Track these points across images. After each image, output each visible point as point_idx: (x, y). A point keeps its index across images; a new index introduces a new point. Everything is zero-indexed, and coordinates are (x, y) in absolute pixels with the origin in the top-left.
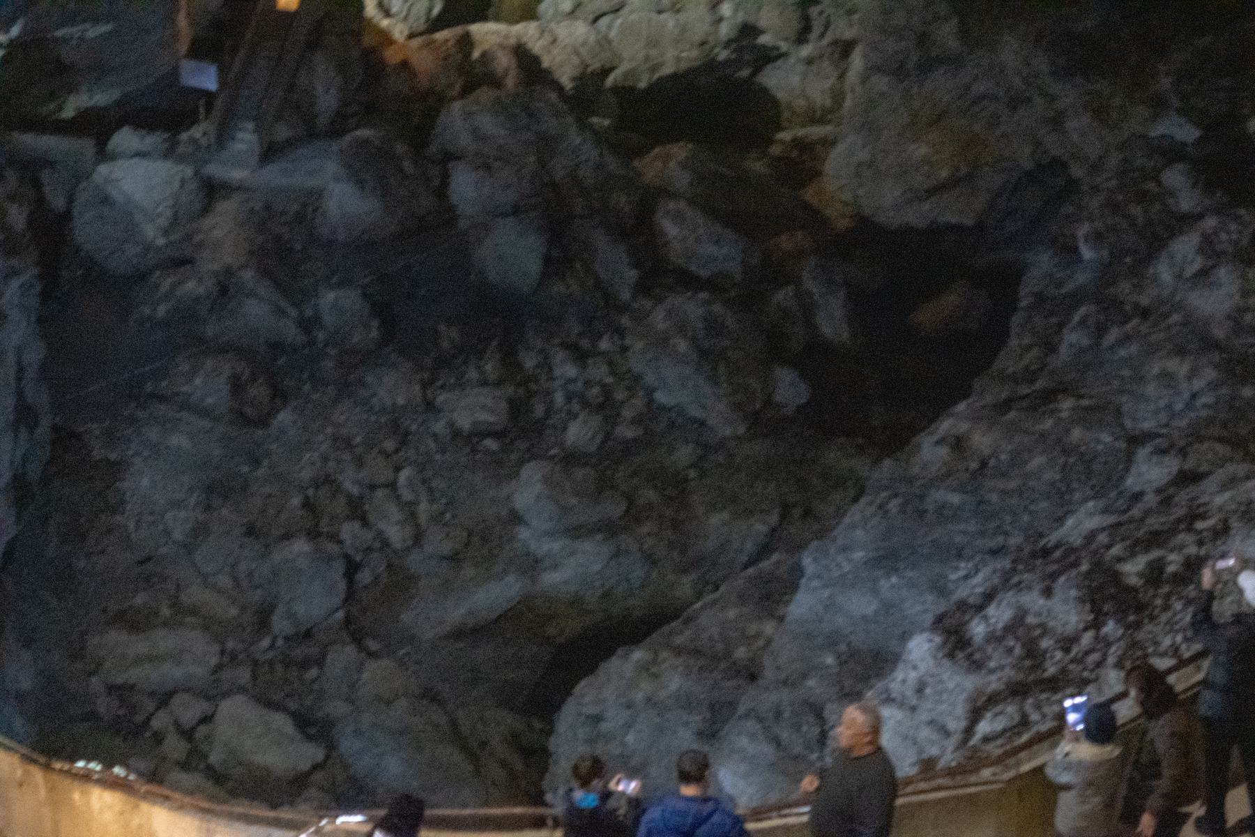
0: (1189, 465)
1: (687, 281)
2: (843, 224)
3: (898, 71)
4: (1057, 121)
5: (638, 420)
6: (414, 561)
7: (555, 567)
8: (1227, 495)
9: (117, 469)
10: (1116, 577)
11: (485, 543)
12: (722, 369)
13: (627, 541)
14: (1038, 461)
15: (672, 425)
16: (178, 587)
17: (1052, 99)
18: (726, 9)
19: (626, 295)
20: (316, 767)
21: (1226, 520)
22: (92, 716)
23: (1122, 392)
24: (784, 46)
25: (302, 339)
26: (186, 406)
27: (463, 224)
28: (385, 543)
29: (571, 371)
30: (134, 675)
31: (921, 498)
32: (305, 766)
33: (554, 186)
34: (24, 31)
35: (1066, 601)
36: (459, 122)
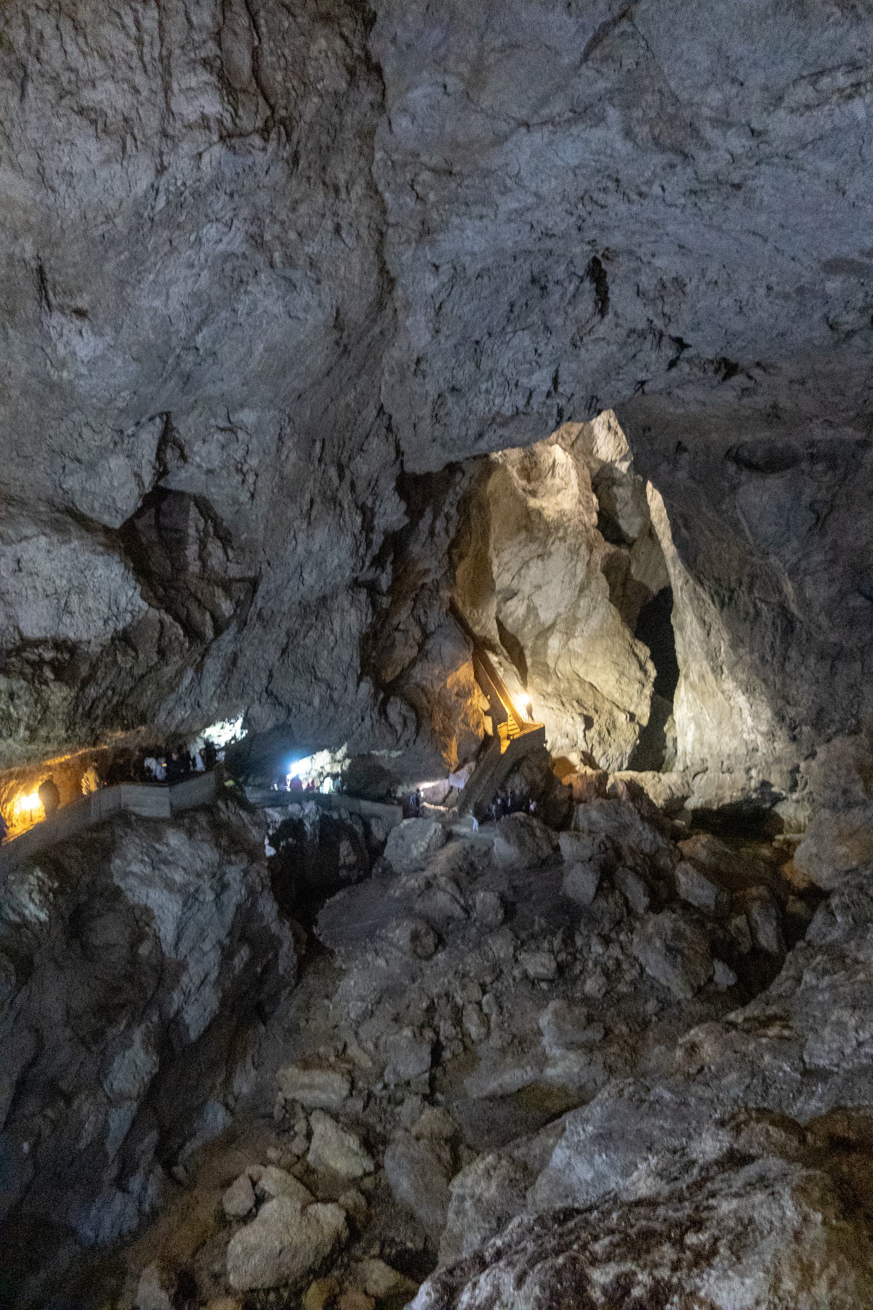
0: (740, 1144)
1: (686, 906)
2: (803, 885)
3: (834, 807)
5: (633, 983)
6: (482, 1050)
7: (554, 1065)
8: (735, 1203)
9: (342, 973)
10: (581, 1283)
11: (522, 1044)
12: (679, 959)
13: (598, 1057)
14: (733, 1076)
15: (652, 987)
16: (345, 1046)
18: (754, 773)
19: (641, 911)
20: (366, 1174)
21: (716, 1240)
22: (271, 1116)
23: (812, 1029)
25: (463, 915)
26: (392, 944)
28: (465, 1034)
29: (600, 950)
30: (300, 1095)
31: (648, 1090)
32: (359, 1172)
33: (617, 850)
35: (527, 1299)
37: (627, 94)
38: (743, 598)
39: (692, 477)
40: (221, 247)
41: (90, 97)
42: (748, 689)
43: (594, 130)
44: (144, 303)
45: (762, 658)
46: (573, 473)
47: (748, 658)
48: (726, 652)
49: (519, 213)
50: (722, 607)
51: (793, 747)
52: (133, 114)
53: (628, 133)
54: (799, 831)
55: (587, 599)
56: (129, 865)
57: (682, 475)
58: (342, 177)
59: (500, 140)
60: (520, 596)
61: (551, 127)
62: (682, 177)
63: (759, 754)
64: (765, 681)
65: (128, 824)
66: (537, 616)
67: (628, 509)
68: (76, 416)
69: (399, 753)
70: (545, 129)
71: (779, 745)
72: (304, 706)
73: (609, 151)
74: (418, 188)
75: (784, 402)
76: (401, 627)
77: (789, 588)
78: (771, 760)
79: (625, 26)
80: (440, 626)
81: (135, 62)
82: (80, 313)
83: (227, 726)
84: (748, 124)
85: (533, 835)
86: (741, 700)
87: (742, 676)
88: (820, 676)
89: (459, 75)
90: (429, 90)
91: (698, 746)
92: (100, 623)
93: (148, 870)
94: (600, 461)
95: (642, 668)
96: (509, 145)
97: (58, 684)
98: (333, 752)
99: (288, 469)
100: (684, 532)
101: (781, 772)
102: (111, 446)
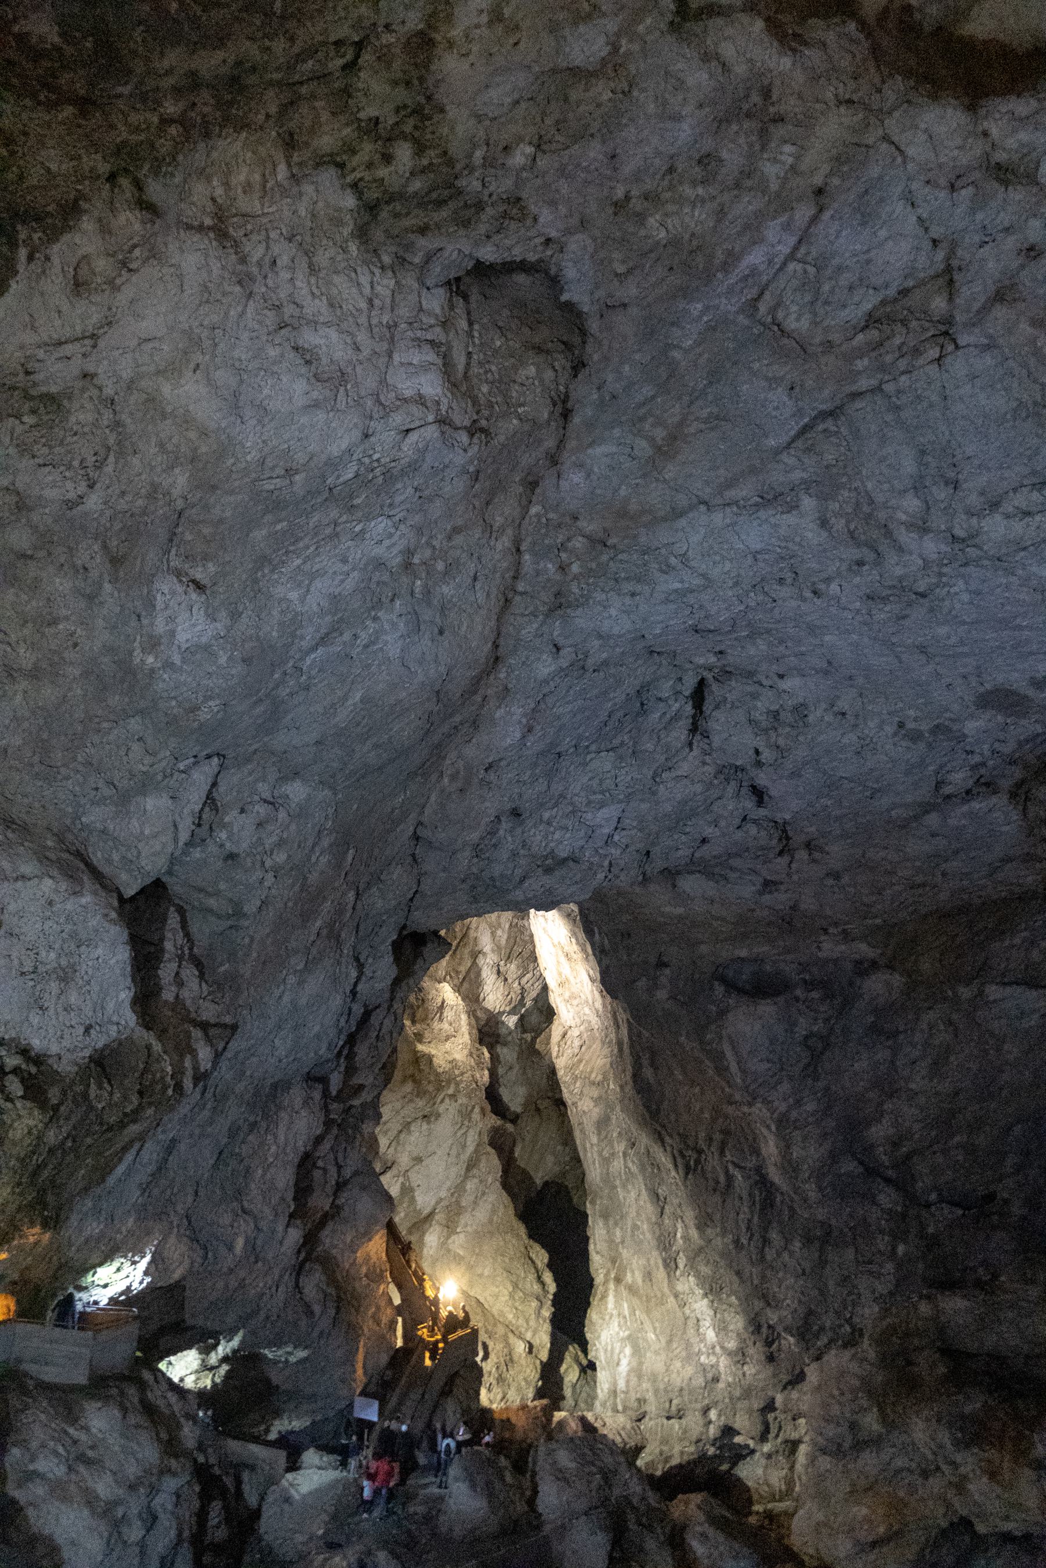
4: (960, 1486)
17: (953, 1464)
18: (713, 1415)
24: (751, 1443)
27: (547, 1528)
34: (242, 1342)
36: (541, 1459)
37: (824, 486)
38: (712, 1162)
39: (673, 998)
40: (379, 551)
41: (309, 338)
42: (713, 1290)
43: (784, 516)
44: (279, 591)
45: (737, 1242)
46: (464, 1017)
47: (718, 1242)
48: (686, 1238)
49: (681, 593)
50: (687, 1174)
51: (769, 1370)
52: (349, 370)
53: (824, 523)
54: (773, 1499)
55: (476, 1181)
56: (32, 1460)
57: (661, 994)
58: (499, 520)
59: (677, 514)
60: (394, 1171)
61: (735, 509)
62: (869, 577)
63: (721, 1385)
64: (738, 1273)
65: (24, 1391)
66: (413, 1200)
67: (513, 1075)
68: (134, 724)
69: (302, 1354)
70: (728, 510)
71: (750, 1370)
72: (223, 1250)
73: (797, 539)
74: (563, 555)
75: (809, 904)
76: (320, 1163)
77: (770, 1148)
78: (737, 1393)
79: (829, 424)
80: (356, 1173)
81: (363, 320)
82: (199, 587)
83: (127, 1268)
84: (949, 530)
85: (502, 1479)
86: (701, 1306)
87: (706, 1270)
88: (807, 1265)
89: (651, 440)
90: (614, 449)
91: (634, 1381)
92: (82, 1030)
93: (61, 1471)
94: (487, 1010)
95: (539, 1279)
96: (683, 522)
97: (28, 1104)
98: (206, 1351)
99: (313, 878)
100: (648, 1073)
101: (750, 1411)
102: (159, 777)
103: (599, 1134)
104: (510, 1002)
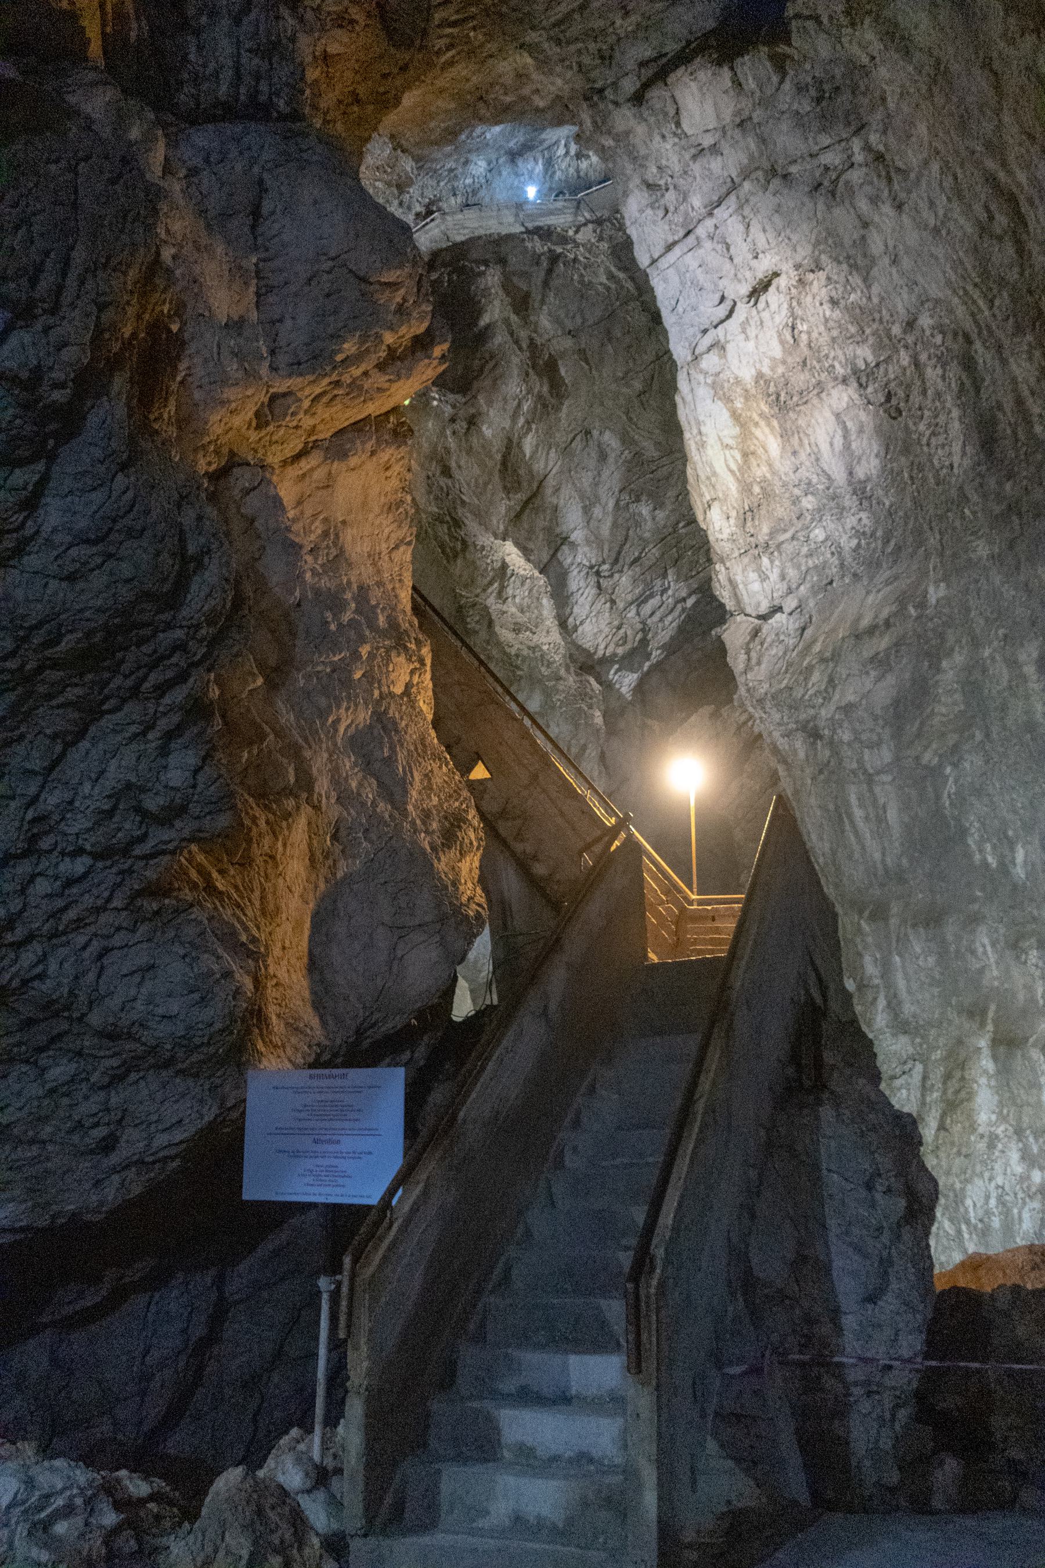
103: (898, 734)
104: (625, 639)
